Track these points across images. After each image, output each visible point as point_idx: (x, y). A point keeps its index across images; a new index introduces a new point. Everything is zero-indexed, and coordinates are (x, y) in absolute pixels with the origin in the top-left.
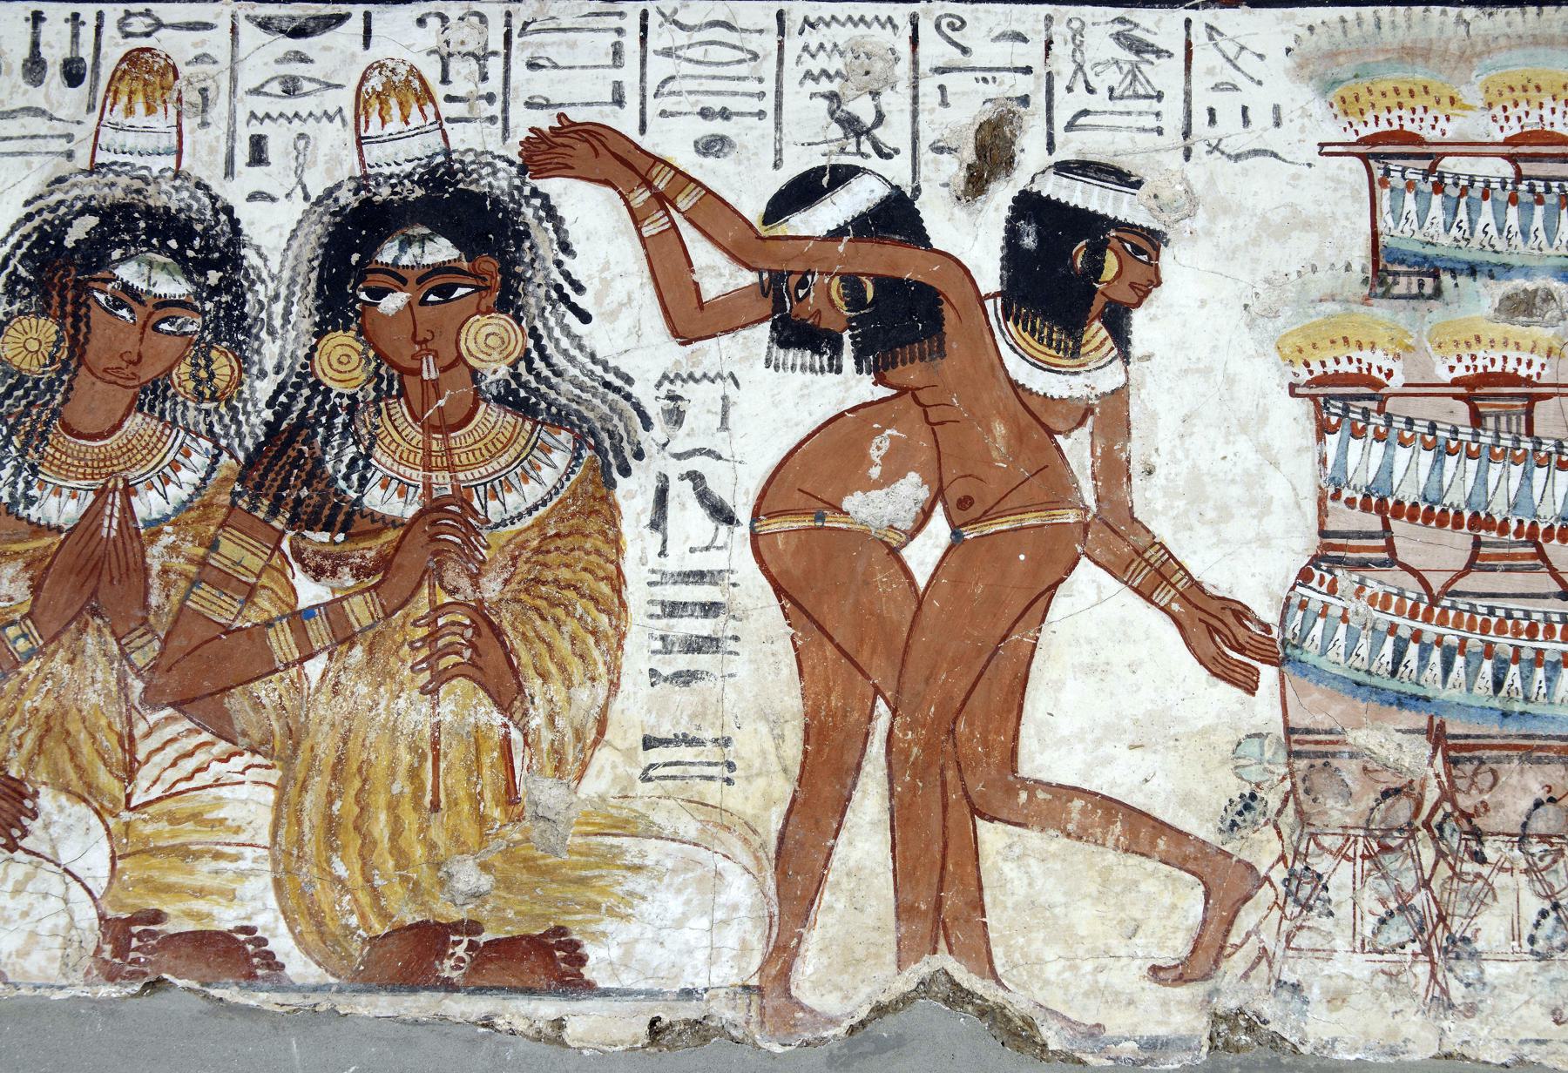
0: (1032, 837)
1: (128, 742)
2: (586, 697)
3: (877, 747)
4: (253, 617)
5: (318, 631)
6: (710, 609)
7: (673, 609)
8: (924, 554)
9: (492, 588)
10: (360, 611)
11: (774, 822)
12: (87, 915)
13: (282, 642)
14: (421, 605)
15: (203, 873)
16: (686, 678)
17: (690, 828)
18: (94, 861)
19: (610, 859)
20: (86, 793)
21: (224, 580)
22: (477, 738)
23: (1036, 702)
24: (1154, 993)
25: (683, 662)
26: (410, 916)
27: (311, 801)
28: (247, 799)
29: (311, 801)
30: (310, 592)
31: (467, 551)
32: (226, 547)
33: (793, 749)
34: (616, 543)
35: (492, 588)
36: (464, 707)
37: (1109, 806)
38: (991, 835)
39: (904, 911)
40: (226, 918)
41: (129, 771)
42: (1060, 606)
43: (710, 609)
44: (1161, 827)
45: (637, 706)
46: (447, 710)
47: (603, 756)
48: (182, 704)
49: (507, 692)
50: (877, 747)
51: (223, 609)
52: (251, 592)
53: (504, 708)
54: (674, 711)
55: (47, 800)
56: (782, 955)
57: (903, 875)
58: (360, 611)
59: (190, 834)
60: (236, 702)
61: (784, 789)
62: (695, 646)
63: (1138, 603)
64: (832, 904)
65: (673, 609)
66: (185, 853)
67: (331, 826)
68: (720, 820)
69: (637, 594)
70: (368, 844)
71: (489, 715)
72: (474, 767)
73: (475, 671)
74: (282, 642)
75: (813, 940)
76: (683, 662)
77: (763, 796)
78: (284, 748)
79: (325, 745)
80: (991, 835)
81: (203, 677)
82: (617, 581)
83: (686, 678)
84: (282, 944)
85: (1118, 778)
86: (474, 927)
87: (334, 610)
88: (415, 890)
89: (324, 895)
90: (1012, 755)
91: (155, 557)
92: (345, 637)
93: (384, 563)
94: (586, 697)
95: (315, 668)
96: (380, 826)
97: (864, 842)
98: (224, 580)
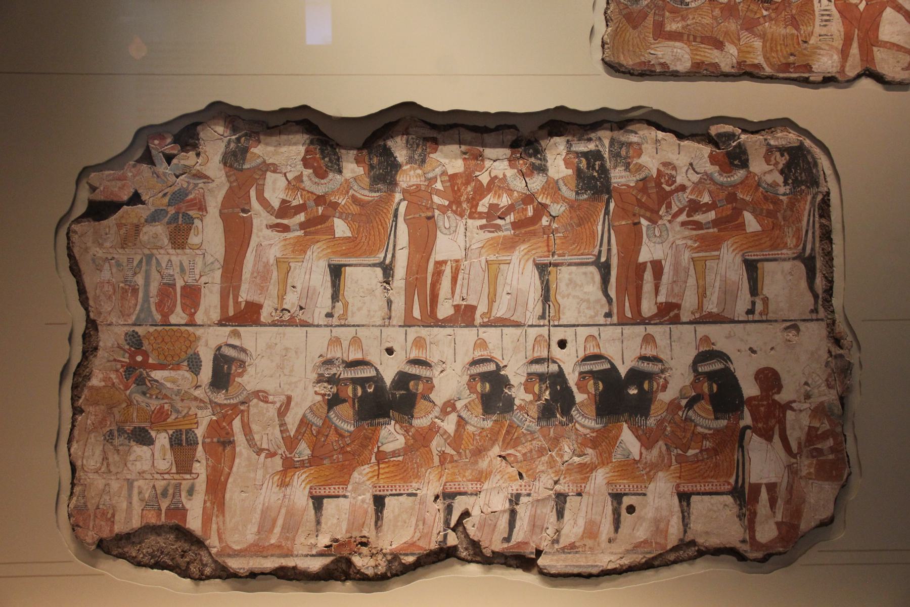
0: (881, 49)
1: (739, 35)
2: (810, 29)
3: (856, 36)
4: (757, 16)
5: (767, 19)
6: (828, 15)
7: (823, 15)
8: (862, 7)
9: (794, 12)
10: (773, 15)
11: (840, 47)
12: (735, 61)
13: (762, 20)
14: (783, 15)
15: (752, 55)
16: (825, 26)
17: (827, 48)
18: (736, 53)
19: (815, 53)
20: (733, 43)
21: (752, 11)
22: (793, 35)
23: (881, 29)
24: (902, 72)
25: (824, 23)
26: (784, 61)
27: (768, 44)
28: (758, 44)
29: (768, 44)
30: (765, 13)
31: (789, 6)
32: (752, 6)
33: (843, 37)
34: (813, 5)
35: (794, 12)
36: (790, 30)
37: (894, 44)
38: (875, 49)
39: (862, 60)
40: (756, 62)
41: (739, 40)
42: (884, 14)
43: (828, 15)
44: (902, 47)
45: (818, 30)
46: (788, 31)
47: (813, 38)
48: (747, 30)
49: (797, 28)
50: (856, 36)
51: (752, 15)
52: (756, 13)
53: (797, 30)
54: (824, 31)
55: (727, 44)
56: (843, 66)
57: (861, 55)
58: (773, 15)
59: (749, 49)
60: (755, 29)
61: (842, 42)
62: (826, 21)
63: (897, 13)
64: (850, 59)
65: (823, 15)
66: (749, 52)
67: (771, 49)
68: (832, 47)
69: (817, 13)
70: (777, 51)
71: (795, 32)
72: (792, 39)
73: (792, 25)
74: (762, 20)
75: (848, 64)
76: (824, 23)
77: (838, 43)
78: (763, 36)
79: (770, 37)
80: (875, 49)
81: (750, 26)
82: (814, 11)
83: (825, 26)
84: (765, 65)
85: (895, 39)
86: (794, 64)
87: (769, 15)
88: (785, 58)
89: (771, 58)
90: (877, 37)
91: (740, 8)
92: (771, 19)
93: (777, 8)
94: (810, 29)
95: (767, 24)
96: (779, 48)
97: (855, 50)
98: (752, 11)
